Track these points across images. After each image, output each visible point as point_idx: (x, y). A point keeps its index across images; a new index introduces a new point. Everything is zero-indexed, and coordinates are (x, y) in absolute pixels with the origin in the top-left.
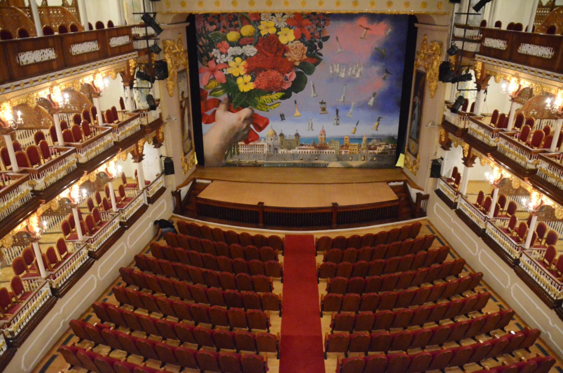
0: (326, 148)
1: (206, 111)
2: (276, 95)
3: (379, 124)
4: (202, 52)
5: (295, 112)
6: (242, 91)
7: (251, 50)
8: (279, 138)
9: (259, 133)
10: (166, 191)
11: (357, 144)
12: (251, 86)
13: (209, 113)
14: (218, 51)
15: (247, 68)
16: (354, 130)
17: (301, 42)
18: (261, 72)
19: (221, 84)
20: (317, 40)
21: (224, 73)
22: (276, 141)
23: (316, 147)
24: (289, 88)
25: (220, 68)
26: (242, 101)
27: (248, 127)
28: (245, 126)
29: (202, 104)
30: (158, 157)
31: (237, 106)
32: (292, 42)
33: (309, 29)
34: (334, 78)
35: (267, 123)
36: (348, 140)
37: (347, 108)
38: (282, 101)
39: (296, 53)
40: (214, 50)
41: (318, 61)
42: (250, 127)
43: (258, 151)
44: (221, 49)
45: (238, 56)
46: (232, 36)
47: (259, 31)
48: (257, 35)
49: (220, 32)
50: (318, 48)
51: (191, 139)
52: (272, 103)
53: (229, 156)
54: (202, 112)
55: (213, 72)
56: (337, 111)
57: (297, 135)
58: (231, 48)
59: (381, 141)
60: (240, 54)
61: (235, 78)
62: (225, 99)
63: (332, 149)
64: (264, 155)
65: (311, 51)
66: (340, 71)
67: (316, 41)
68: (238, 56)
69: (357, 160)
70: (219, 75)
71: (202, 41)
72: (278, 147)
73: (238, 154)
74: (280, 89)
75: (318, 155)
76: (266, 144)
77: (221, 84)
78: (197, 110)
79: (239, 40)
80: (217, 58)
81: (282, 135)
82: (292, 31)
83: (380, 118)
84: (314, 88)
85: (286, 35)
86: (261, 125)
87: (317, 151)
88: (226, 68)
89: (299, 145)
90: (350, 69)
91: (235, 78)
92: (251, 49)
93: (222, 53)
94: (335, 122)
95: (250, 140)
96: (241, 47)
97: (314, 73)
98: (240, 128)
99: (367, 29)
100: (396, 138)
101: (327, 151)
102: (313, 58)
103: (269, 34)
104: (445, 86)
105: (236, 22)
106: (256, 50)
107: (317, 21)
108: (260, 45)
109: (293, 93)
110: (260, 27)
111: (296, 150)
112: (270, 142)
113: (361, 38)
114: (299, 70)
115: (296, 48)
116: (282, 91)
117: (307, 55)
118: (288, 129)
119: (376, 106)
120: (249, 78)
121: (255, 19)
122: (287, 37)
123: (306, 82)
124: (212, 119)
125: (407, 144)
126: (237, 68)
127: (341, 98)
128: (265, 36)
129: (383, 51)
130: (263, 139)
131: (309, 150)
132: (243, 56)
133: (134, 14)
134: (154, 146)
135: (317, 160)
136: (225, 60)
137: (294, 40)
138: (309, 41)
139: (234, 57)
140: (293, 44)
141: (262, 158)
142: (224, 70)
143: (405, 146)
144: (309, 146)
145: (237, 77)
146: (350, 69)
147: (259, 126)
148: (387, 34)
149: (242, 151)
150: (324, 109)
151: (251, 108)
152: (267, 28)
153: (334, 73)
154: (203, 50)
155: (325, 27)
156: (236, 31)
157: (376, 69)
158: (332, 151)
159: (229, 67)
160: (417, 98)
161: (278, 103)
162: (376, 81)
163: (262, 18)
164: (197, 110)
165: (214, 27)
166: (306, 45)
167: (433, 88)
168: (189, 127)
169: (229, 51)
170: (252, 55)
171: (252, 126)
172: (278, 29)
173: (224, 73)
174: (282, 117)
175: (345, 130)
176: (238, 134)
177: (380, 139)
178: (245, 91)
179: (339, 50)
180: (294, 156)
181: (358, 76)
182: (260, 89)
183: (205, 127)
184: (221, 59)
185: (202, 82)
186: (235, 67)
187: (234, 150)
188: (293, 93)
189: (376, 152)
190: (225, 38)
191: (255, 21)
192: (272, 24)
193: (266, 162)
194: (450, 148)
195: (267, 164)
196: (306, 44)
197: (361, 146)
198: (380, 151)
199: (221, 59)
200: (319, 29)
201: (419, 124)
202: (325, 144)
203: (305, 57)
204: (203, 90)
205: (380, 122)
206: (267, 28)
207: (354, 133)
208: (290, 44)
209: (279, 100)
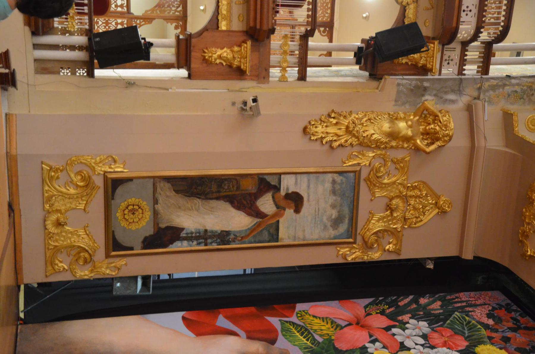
1: (226, 317)
54: (221, 310)
55: (358, 323)
88: (385, 347)
185: (316, 306)
204: (294, 308)
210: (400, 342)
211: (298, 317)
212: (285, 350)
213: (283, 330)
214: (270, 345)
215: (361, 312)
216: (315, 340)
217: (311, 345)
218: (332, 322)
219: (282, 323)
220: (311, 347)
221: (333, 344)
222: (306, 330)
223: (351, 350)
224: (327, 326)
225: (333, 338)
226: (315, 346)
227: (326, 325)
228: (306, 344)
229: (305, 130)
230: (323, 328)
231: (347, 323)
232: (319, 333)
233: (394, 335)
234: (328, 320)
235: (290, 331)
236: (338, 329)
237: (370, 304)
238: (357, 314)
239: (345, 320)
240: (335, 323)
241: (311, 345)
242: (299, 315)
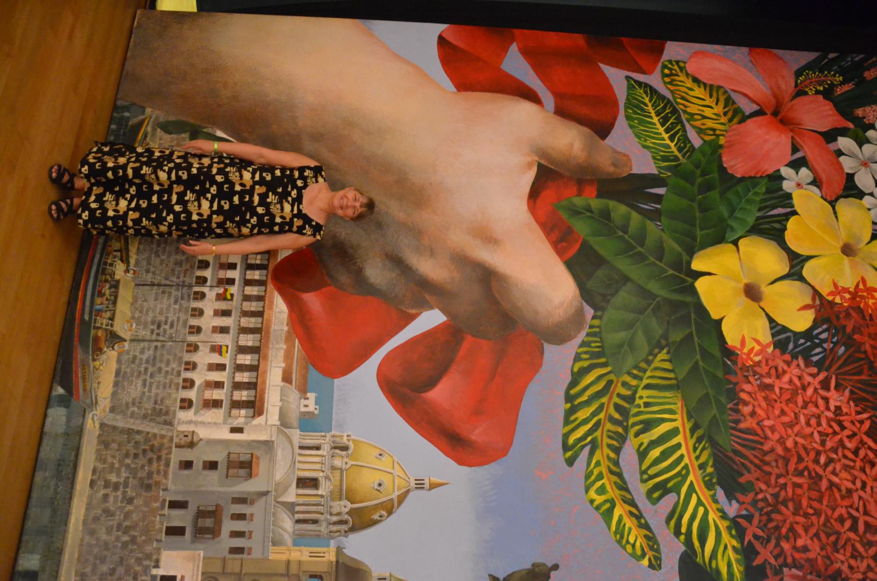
1: (526, 53)
12: (744, 330)
18: (854, 398)
19: (714, 149)
21: (785, 171)
22: (287, 523)
26: (623, 265)
27: (426, 292)
28: (430, 268)
31: (582, 228)
35: (454, 442)
42: (424, 305)
43: (204, 357)
52: (639, 490)
54: (517, 32)
55: (777, 113)
62: (623, 159)
64: (161, 414)
72: (226, 542)
74: (765, 555)
76: (260, 429)
77: (714, 149)
86: (440, 394)
88: (816, 182)
91: (772, 230)
95: (312, 300)
98: (417, 233)
112: (279, 471)
130: (311, 404)
141: (135, 390)
142: (804, 171)
145: (782, 243)
147: (432, 383)
151: (577, 318)
159: (833, 203)
171: (431, 319)
173: (785, 171)
178: (701, 285)
182: (733, 394)
184: (865, 164)
185: (704, 53)
186: (844, 237)
193: (92, 426)
195: (74, 436)
204: (661, 51)
209: (672, 550)
210: (847, 174)
211: (664, 76)
212: (624, 155)
213: (629, 104)
214: (598, 138)
215: (787, 84)
216: (686, 139)
217: (677, 153)
218: (729, 101)
219: (633, 84)
220: (676, 159)
221: (720, 157)
222: (675, 111)
223: (751, 177)
224: (715, 111)
225: (722, 141)
226: (683, 156)
227: (713, 105)
228: (669, 147)
230: (708, 112)
231: (755, 108)
232: (697, 123)
233: (839, 153)
234: (720, 92)
235: (643, 110)
236: (735, 120)
237: (809, 66)
238: (779, 88)
239: (753, 101)
240: (734, 103)
241: (677, 153)
242: (666, 71)
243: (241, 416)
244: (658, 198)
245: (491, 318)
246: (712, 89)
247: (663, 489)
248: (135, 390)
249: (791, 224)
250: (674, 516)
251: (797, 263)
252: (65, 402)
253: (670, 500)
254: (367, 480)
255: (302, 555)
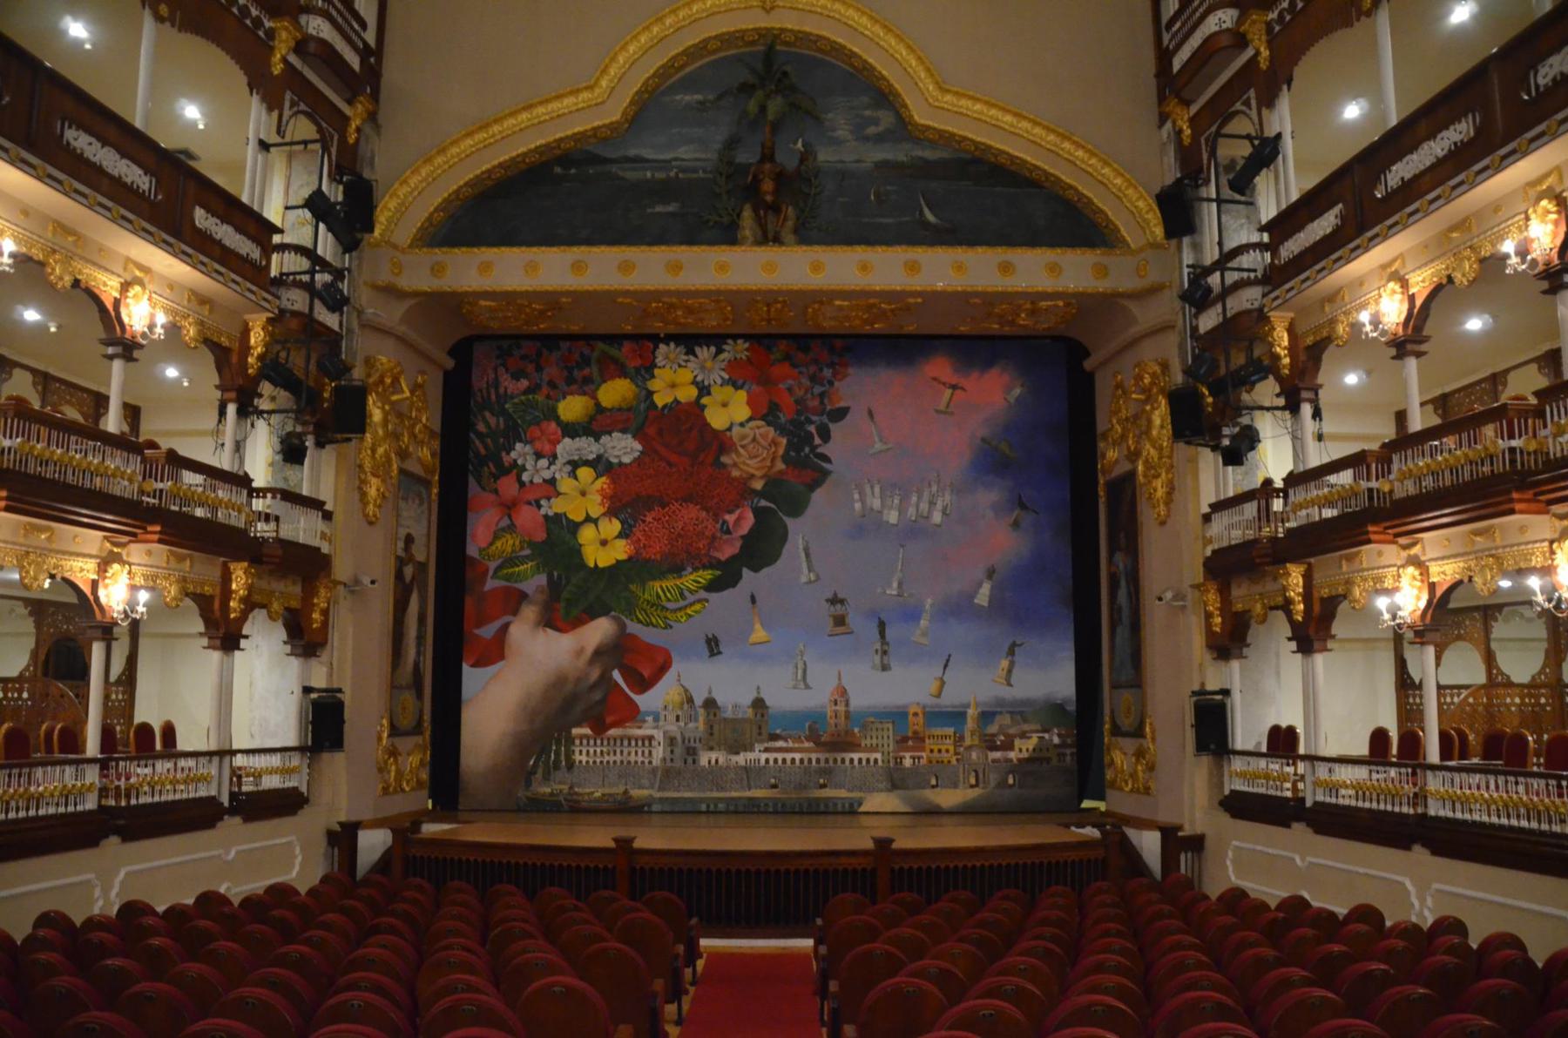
0: (853, 746)
1: (479, 625)
2: (694, 579)
3: (1012, 664)
4: (483, 451)
5: (751, 630)
6: (592, 565)
7: (623, 447)
8: (701, 711)
9: (638, 699)
10: (305, 815)
11: (950, 731)
12: (620, 551)
13: (488, 631)
14: (528, 448)
15: (611, 498)
16: (938, 683)
17: (769, 424)
19: (531, 544)
20: (814, 418)
21: (543, 511)
22: (691, 725)
23: (820, 745)
24: (733, 557)
25: (531, 497)
27: (605, 678)
28: (595, 674)
29: (469, 602)
30: (298, 691)
31: (575, 612)
32: (742, 425)
33: (790, 389)
34: (866, 527)
35: (664, 668)
36: (921, 719)
37: (912, 615)
38: (713, 596)
39: (754, 451)
40: (518, 446)
41: (819, 477)
42: (611, 678)
43: (633, 758)
44: (538, 445)
45: (587, 463)
46: (572, 407)
47: (650, 393)
48: (643, 406)
49: (540, 398)
50: (817, 441)
51: (420, 696)
52: (682, 603)
53: (539, 775)
55: (509, 507)
56: (882, 626)
57: (759, 704)
58: (567, 440)
59: (1025, 721)
60: (591, 457)
61: (575, 527)
63: (873, 749)
64: (654, 771)
65: (799, 450)
66: (883, 505)
67: (812, 423)
68: (587, 463)
69: (955, 785)
70: (526, 517)
71: (486, 422)
72: (698, 745)
73: (571, 765)
75: (826, 772)
76: (659, 735)
77: (531, 544)
78: (450, 618)
79: (592, 419)
80: (524, 469)
81: (710, 704)
82: (742, 395)
83: (1014, 645)
84: (807, 555)
85: (725, 405)
86: (646, 673)
87: (822, 756)
88: (549, 499)
89: (765, 736)
90: (914, 499)
91: (575, 527)
92: (623, 444)
93: (539, 455)
94: (877, 659)
95: (609, 720)
96: (597, 439)
97: (810, 511)
98: (579, 680)
99: (954, 387)
100: (1072, 708)
101: (856, 756)
102: (804, 470)
103: (676, 401)
104: (1194, 461)
105: (587, 371)
106: (640, 447)
107: (812, 369)
108: (651, 431)
109: (745, 571)
110: (654, 385)
111: (758, 755)
112: (673, 728)
113: (938, 411)
114: (763, 503)
115: (754, 440)
116: (711, 567)
117: (785, 458)
118: (731, 684)
119: (998, 604)
120: (616, 526)
121: (639, 362)
122: (729, 410)
123: (784, 538)
124: (494, 652)
125: (1107, 711)
126: (581, 498)
127: (890, 586)
128: (665, 406)
129: (1004, 447)
130: (650, 719)
131: (797, 754)
132: (600, 465)
133: (287, 208)
134: (288, 648)
135: (823, 786)
136: (547, 475)
137: (750, 419)
138: (792, 421)
139: (574, 465)
140: (746, 430)
141: (645, 782)
142: (543, 502)
143: (1102, 724)
144: (799, 739)
146: (914, 499)
148: (1012, 401)
149: (584, 758)
150: (840, 621)
151: (614, 618)
152: (673, 386)
153: (867, 512)
154: (486, 447)
155: (836, 384)
156: (584, 394)
157: (988, 497)
158: (873, 756)
159: (559, 494)
160: (1119, 558)
161: (699, 601)
162: (994, 537)
163: (659, 360)
164: (450, 618)
165: (524, 383)
166: (782, 434)
167: (1160, 493)
168: (419, 652)
169: (559, 449)
170: (627, 460)
172: (704, 390)
173: (543, 511)
174: (713, 646)
175: (906, 686)
176: (570, 701)
177: (1021, 711)
178: (601, 565)
179: (878, 446)
180: (750, 774)
181: (937, 517)
182: (647, 561)
183: (471, 677)
187: (557, 754)
188: (745, 571)
189: (1012, 755)
190: (552, 414)
191: (637, 370)
192: (686, 375)
193: (658, 795)
194: (1245, 650)
195: (661, 799)
196: (782, 430)
197: (962, 738)
198: (1025, 755)
199: (536, 471)
200: (818, 390)
201: (1136, 627)
202: (847, 732)
203: (780, 466)
204: (472, 559)
205: (1017, 658)
206: (673, 386)
207: (939, 696)
208: (736, 430)
209: (703, 594)
215: (492, 497)
216: (527, 557)
218: (503, 530)
219: (495, 576)
229: (371, 523)
237: (479, 483)
243: (654, 743)
244: (560, 577)
245: (620, 651)
246: (496, 537)
247: (682, 594)
248: (645, 782)
249: (571, 517)
250: (691, 592)
251: (588, 519)
252: (649, 805)
253: (687, 593)
254: (677, 699)
255: (701, 719)
